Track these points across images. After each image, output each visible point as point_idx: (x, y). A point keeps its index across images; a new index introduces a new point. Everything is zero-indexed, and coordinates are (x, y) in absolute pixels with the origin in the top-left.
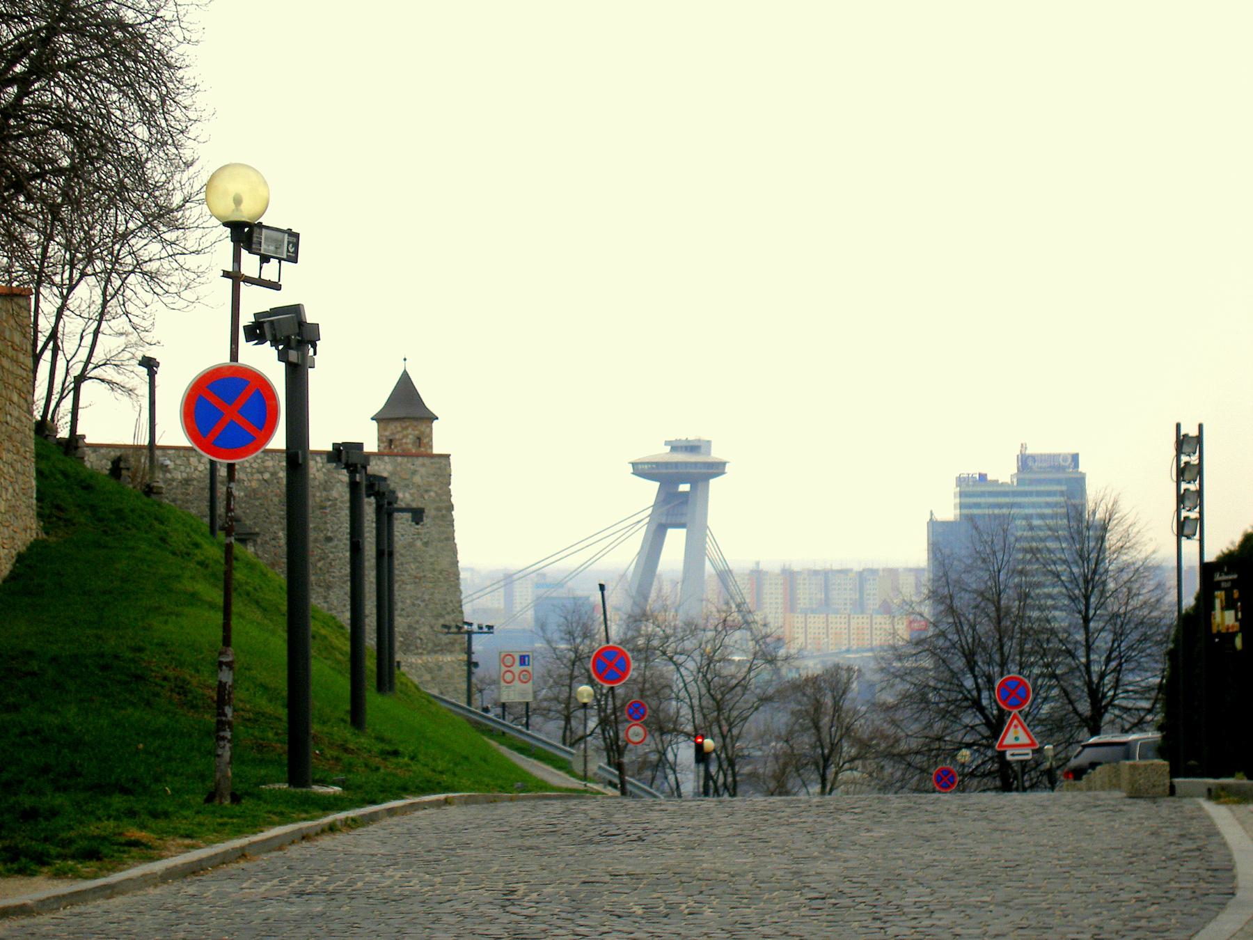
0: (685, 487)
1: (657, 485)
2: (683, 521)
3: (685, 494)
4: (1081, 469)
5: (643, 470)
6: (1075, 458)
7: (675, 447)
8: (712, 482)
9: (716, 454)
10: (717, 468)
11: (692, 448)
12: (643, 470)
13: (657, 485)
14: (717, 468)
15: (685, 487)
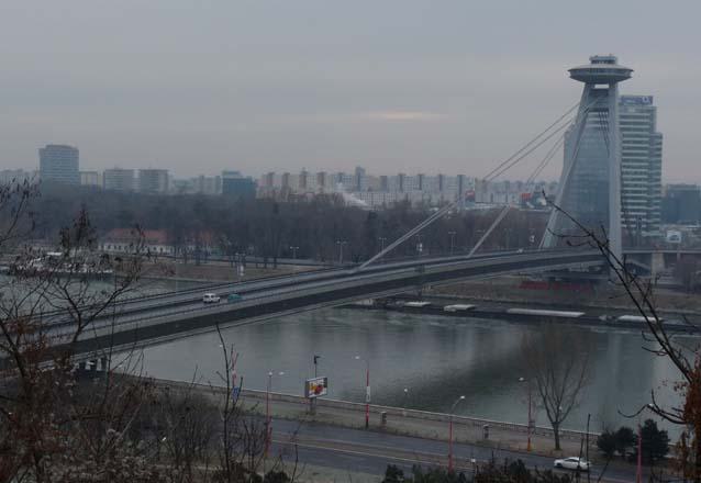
0: (606, 86)
1: (583, 84)
2: (604, 106)
3: (606, 90)
4: (654, 105)
5: (577, 74)
6: (651, 98)
7: (594, 62)
8: (620, 83)
9: (621, 64)
10: (624, 74)
11: (610, 61)
12: (577, 74)
13: (583, 84)
14: (624, 74)
15: (606, 86)
